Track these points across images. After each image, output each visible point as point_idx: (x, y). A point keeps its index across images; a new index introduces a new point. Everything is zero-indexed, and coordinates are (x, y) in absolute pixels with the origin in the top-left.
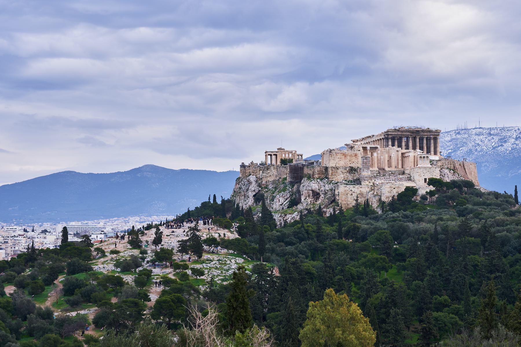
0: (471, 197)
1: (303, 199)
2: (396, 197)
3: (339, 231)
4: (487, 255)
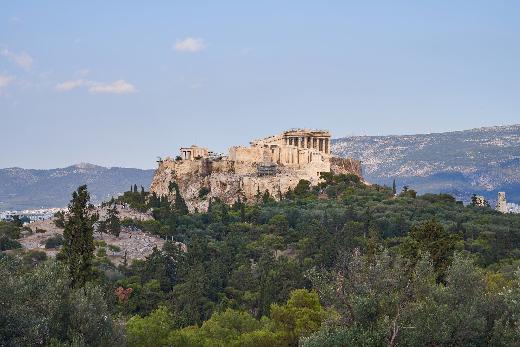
1: (212, 189)
3: (242, 215)
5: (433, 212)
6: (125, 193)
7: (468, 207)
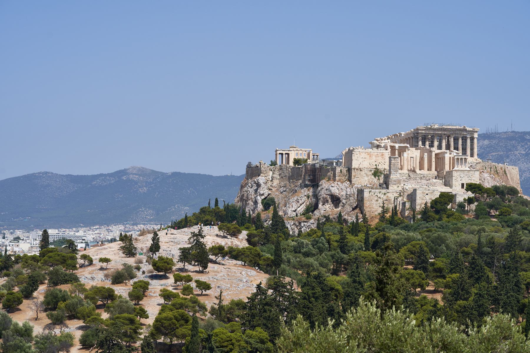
1: (320, 206)
2: (429, 205)
6: (201, 209)
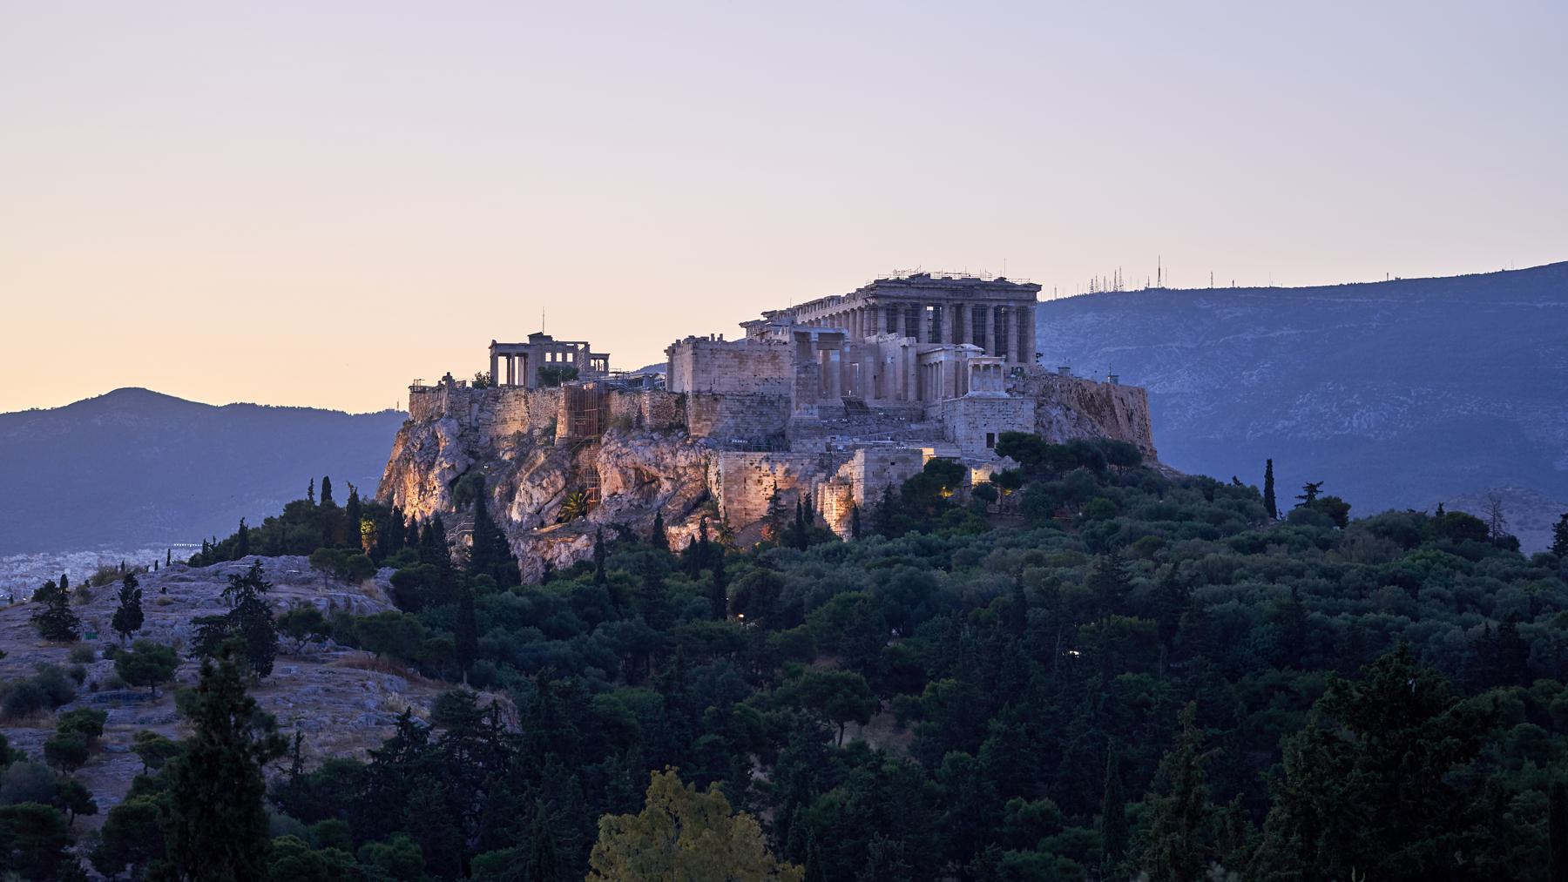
0: (1129, 494)
2: (898, 492)
4: (1179, 672)
5: (1409, 583)
6: (289, 507)
7: (1541, 560)
